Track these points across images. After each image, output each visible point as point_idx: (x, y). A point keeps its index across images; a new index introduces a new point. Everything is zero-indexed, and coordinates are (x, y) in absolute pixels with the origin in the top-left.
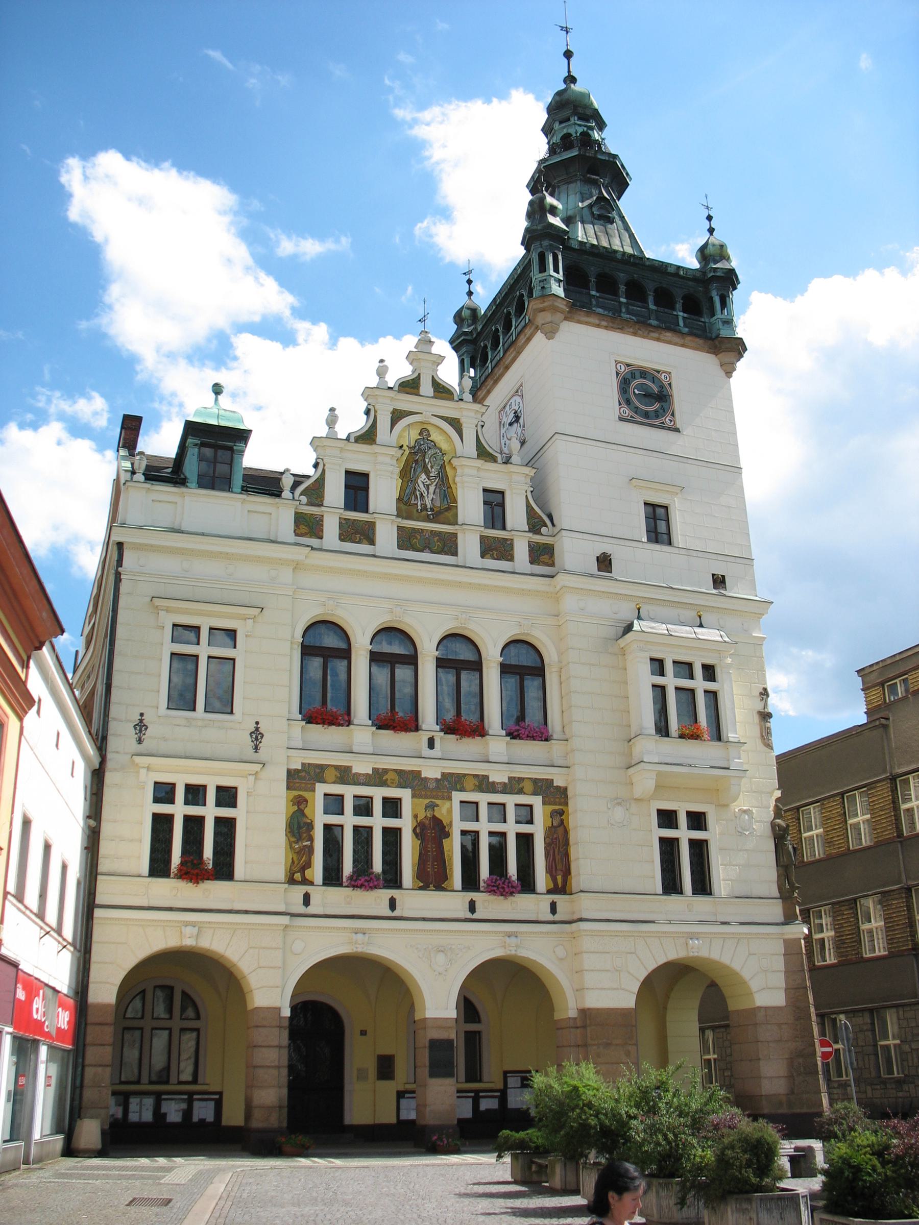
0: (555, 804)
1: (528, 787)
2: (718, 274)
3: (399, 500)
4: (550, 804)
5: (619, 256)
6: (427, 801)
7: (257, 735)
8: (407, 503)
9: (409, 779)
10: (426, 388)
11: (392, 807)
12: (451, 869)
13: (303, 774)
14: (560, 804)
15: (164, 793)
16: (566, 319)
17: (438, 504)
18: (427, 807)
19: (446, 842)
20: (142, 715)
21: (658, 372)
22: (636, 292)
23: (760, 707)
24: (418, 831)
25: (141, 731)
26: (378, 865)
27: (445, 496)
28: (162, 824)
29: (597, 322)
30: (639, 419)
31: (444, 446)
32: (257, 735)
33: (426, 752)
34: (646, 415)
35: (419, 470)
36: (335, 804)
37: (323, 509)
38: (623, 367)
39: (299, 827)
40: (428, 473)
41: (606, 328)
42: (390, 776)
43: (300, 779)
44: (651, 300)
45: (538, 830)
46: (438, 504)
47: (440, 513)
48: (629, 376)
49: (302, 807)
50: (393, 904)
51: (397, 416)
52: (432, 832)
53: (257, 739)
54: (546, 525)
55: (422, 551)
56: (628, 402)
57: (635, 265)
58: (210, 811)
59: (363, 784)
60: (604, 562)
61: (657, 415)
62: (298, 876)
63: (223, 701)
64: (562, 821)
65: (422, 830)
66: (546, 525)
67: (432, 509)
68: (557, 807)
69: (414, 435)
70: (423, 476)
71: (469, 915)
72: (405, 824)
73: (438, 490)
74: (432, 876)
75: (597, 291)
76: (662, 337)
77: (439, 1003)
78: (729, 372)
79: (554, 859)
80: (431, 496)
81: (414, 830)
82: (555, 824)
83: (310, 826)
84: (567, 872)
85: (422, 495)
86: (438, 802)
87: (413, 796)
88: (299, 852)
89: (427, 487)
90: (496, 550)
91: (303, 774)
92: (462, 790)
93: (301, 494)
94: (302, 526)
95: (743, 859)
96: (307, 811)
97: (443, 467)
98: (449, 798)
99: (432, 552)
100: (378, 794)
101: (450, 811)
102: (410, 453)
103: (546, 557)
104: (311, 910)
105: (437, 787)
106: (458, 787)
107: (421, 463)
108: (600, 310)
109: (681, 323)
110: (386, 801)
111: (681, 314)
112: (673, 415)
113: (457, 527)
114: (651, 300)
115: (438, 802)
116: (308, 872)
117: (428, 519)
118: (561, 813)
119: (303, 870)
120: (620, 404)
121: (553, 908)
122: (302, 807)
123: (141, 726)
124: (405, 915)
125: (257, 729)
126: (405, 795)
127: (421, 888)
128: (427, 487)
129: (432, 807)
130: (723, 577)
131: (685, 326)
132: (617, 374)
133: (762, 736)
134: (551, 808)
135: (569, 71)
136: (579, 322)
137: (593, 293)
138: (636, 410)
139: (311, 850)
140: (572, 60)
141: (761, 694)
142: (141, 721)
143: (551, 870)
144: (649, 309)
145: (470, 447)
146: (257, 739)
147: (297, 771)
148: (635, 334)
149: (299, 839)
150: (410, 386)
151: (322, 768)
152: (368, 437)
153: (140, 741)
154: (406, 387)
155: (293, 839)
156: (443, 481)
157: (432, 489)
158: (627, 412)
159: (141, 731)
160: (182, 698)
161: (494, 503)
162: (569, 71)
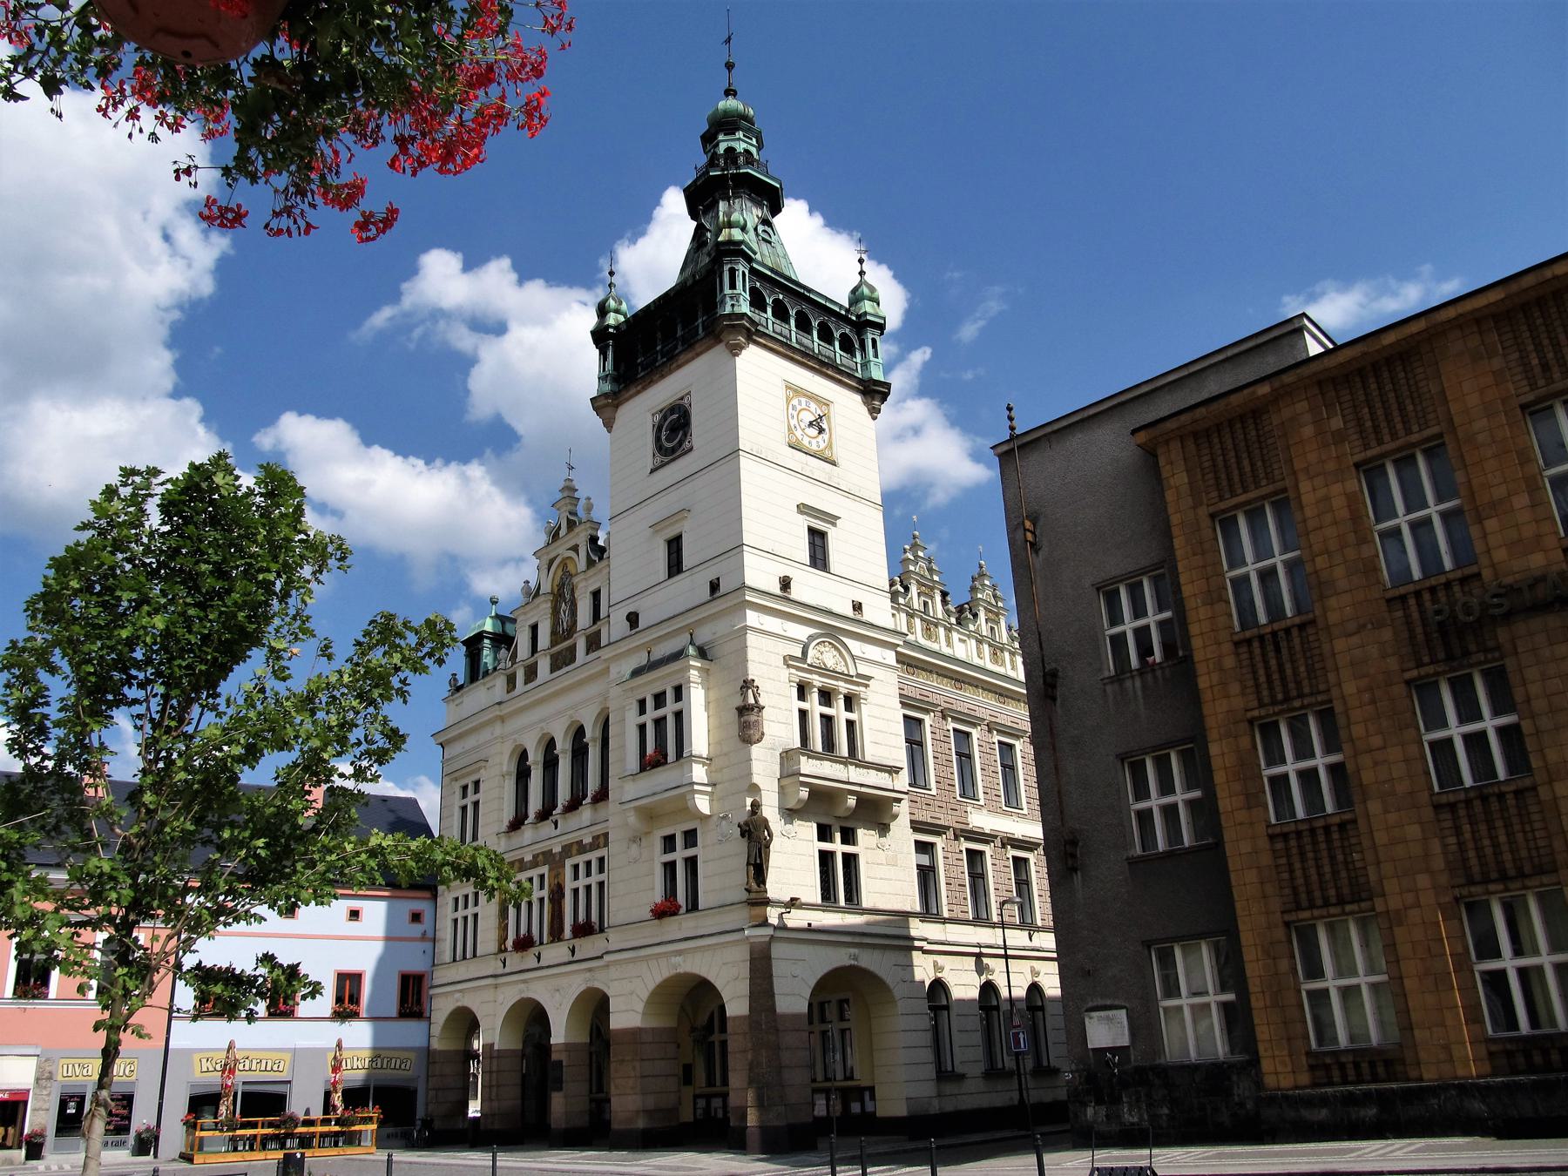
10: (562, 532)
16: (617, 407)
23: (738, 702)
30: (666, 459)
34: (673, 450)
41: (644, 389)
60: (633, 619)
69: (560, 573)
72: (545, 893)
74: (556, 934)
136: (627, 400)
148: (663, 377)
158: (659, 459)
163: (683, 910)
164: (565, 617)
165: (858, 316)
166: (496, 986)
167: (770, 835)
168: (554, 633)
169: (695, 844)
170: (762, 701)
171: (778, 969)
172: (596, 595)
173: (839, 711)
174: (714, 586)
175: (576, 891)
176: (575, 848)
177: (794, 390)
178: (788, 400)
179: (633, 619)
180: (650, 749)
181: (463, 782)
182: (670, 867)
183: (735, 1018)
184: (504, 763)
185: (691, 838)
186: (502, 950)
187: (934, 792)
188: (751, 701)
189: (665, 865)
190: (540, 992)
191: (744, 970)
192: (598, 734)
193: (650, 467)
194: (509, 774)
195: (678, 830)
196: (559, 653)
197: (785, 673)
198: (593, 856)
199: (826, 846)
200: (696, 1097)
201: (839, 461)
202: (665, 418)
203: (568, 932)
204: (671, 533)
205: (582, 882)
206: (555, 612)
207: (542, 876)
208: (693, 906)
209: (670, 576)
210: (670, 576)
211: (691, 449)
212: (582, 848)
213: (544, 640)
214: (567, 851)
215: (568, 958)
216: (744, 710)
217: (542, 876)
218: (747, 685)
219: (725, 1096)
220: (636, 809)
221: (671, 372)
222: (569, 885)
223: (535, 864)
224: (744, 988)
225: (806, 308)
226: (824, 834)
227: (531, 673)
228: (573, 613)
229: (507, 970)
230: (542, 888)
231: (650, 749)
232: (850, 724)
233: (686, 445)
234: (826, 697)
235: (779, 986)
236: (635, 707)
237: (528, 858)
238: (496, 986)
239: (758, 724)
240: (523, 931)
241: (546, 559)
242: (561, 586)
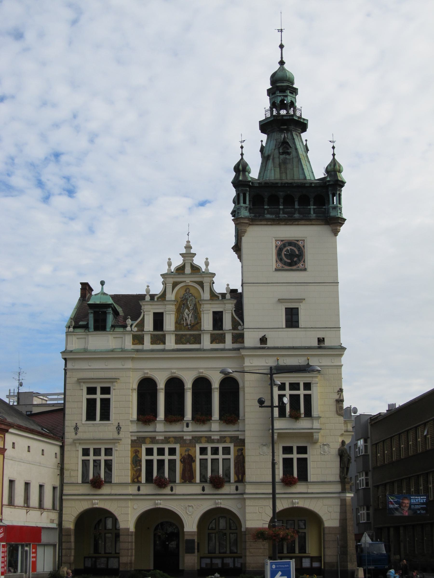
0: (240, 446)
1: (228, 440)
2: (331, 183)
3: (176, 323)
4: (237, 446)
5: (279, 185)
6: (186, 448)
7: (119, 428)
8: (179, 324)
9: (179, 440)
10: (188, 270)
11: (172, 451)
12: (195, 474)
13: (137, 441)
14: (242, 446)
15: (86, 452)
16: (250, 225)
17: (193, 322)
18: (186, 451)
19: (193, 464)
20: (76, 424)
21: (298, 241)
22: (289, 201)
23: (337, 397)
24: (182, 460)
25: (76, 430)
26: (166, 475)
27: (196, 318)
28: (85, 464)
29: (266, 223)
31: (196, 295)
32: (119, 428)
33: (185, 429)
35: (185, 308)
36: (149, 452)
37: (143, 332)
38: (279, 243)
39: (136, 461)
40: (188, 309)
41: (271, 225)
42: (172, 439)
43: (136, 443)
44: (296, 203)
45: (232, 457)
46: (193, 322)
47: (193, 326)
48: (282, 247)
49: (137, 454)
50: (172, 490)
51: (175, 285)
52: (188, 461)
53: (119, 429)
54: (240, 325)
55: (186, 344)
56: (281, 260)
58: (103, 458)
59: (161, 443)
60: (263, 340)
61: (296, 263)
62: (136, 480)
63: (105, 416)
64: (242, 454)
65: (184, 460)
66: (240, 325)
67: (190, 325)
68: (240, 448)
69: (182, 292)
70: (187, 310)
71: (202, 492)
72: (177, 457)
73: (193, 316)
74: (188, 477)
75: (268, 206)
76: (299, 223)
77: (190, 525)
78: (336, 233)
79: (238, 468)
80: (190, 319)
81: (181, 460)
82: (239, 454)
83: (140, 461)
84: (244, 473)
85: (186, 319)
86: (190, 448)
87: (181, 447)
88: (136, 471)
89: (188, 315)
90: (217, 338)
91: (137, 441)
92: (201, 443)
93: (135, 326)
94: (136, 340)
95: (323, 465)
96: (139, 455)
97: (195, 305)
98: (195, 447)
99: (190, 344)
101: (195, 452)
102: (181, 301)
103: (241, 339)
104: (141, 492)
105: (190, 442)
106: (199, 442)
107: (186, 304)
108: (268, 216)
109: (312, 212)
110: (170, 449)
111: (312, 207)
112: (304, 262)
113: (200, 332)
114: (296, 203)
115: (190, 448)
116: (139, 479)
117: (189, 330)
118: (242, 450)
119: (137, 478)
120: (277, 262)
121: (237, 489)
122: (137, 454)
123: (76, 428)
124: (177, 493)
125: (119, 426)
126: (177, 447)
127: (183, 483)
128: (188, 315)
129: (188, 450)
130: (323, 338)
131: (314, 213)
132: (276, 246)
133: (337, 411)
134: (237, 448)
135: (282, 58)
137: (266, 207)
138: (285, 264)
139: (140, 470)
140: (284, 49)
141: (338, 391)
142: (76, 426)
143: (236, 473)
144: (295, 208)
145: (206, 295)
146: (119, 429)
147: (135, 440)
149: (136, 466)
150: (181, 269)
152: (163, 296)
153: (76, 434)
154: (179, 270)
155: (134, 466)
156: (195, 311)
157: (190, 315)
159: (76, 430)
160: (91, 416)
161: (218, 318)
162: (282, 58)
166: (131, 499)
168: (179, 323)
169: (306, 453)
174: (321, 341)
179: (263, 340)
183: (329, 528)
189: (284, 459)
193: (274, 267)
196: (182, 335)
202: (284, 245)
206: (179, 312)
211: (305, 270)
214: (196, 439)
215: (201, 492)
223: (167, 440)
227: (159, 339)
233: (300, 265)
241: (171, 281)
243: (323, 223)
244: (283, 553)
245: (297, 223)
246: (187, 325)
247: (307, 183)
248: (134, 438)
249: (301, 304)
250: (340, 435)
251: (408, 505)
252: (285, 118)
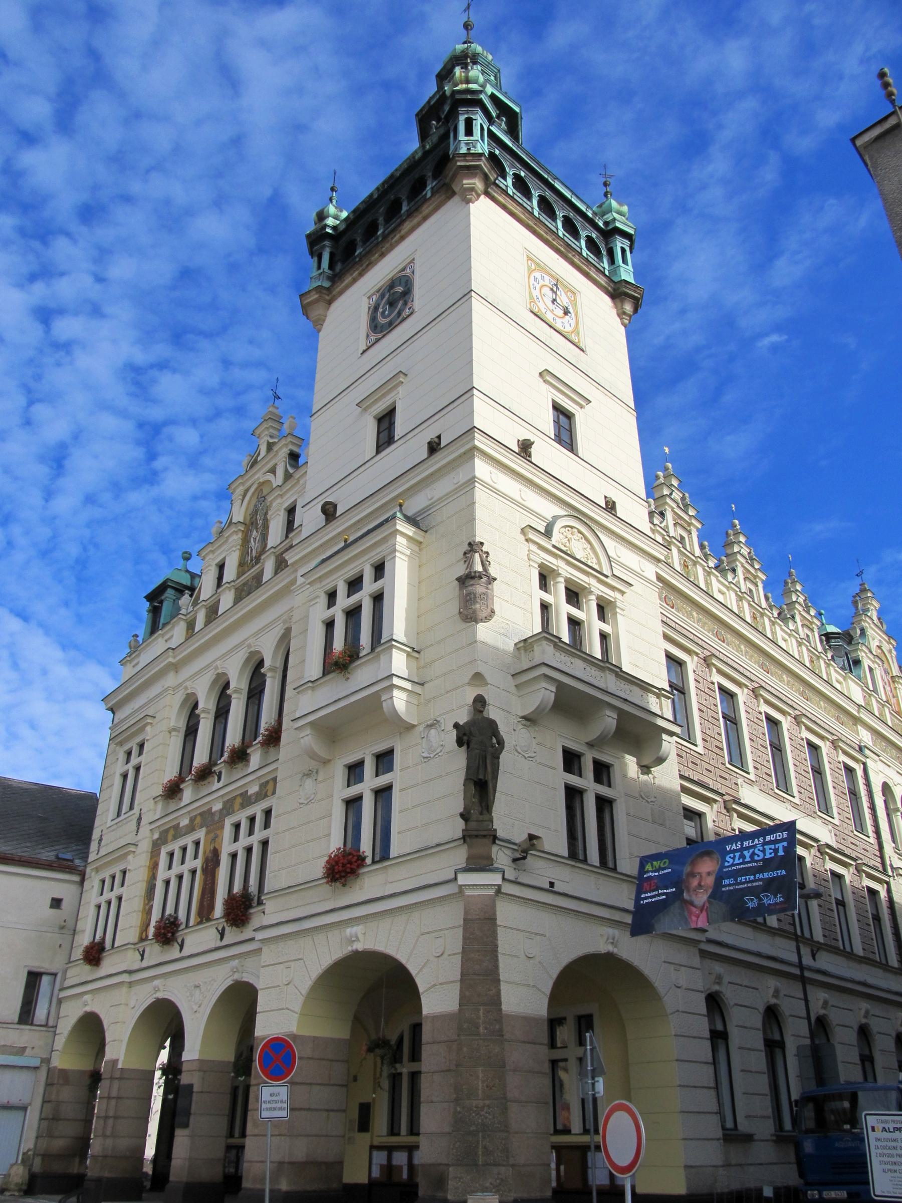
5: (375, 196)
16: (330, 303)
21: (404, 269)
23: (461, 571)
40: (257, 529)
41: (361, 275)
57: (391, 187)
76: (403, 232)
100: (188, 840)
123: (101, 840)
128: (255, 539)
136: (341, 293)
141: (465, 553)
148: (383, 255)
151: (166, 831)
163: (369, 861)
164: (254, 545)
165: (606, 223)
166: (131, 984)
167: (501, 743)
169: (390, 769)
170: (492, 571)
171: (505, 941)
172: (291, 511)
173: (588, 614)
175: (234, 856)
176: (239, 800)
177: (534, 264)
178: (530, 272)
179: (329, 512)
180: (339, 644)
181: (127, 747)
182: (353, 804)
183: (434, 1018)
184: (171, 717)
185: (384, 760)
186: (143, 939)
187: (700, 749)
188: (479, 568)
190: (177, 991)
191: (454, 941)
192: (279, 664)
194: (174, 729)
195: (365, 751)
197: (524, 548)
198: (257, 810)
199: (574, 780)
200: (372, 1147)
201: (588, 350)
203: (219, 910)
204: (381, 407)
205: (244, 841)
206: (246, 541)
207: (197, 844)
208: (383, 853)
209: (379, 449)
210: (379, 449)
212: (247, 800)
213: (230, 574)
216: (467, 579)
217: (197, 844)
218: (473, 547)
219: (411, 1149)
220: (312, 724)
221: (392, 247)
222: (227, 848)
224: (452, 968)
225: (549, 194)
226: (571, 760)
228: (264, 537)
229: (145, 964)
230: (196, 857)
231: (339, 644)
232: (604, 636)
234: (574, 596)
235: (508, 969)
236: (323, 600)
237: (185, 822)
238: (131, 984)
239: (487, 597)
240: (169, 910)
242: (255, 512)
243: (443, 197)
244: (567, 1131)
245: (398, 236)
246: (252, 560)
247: (416, 152)
248: (156, 836)
249: (400, 389)
250: (467, 680)
251: (710, 881)
252: (432, 103)
